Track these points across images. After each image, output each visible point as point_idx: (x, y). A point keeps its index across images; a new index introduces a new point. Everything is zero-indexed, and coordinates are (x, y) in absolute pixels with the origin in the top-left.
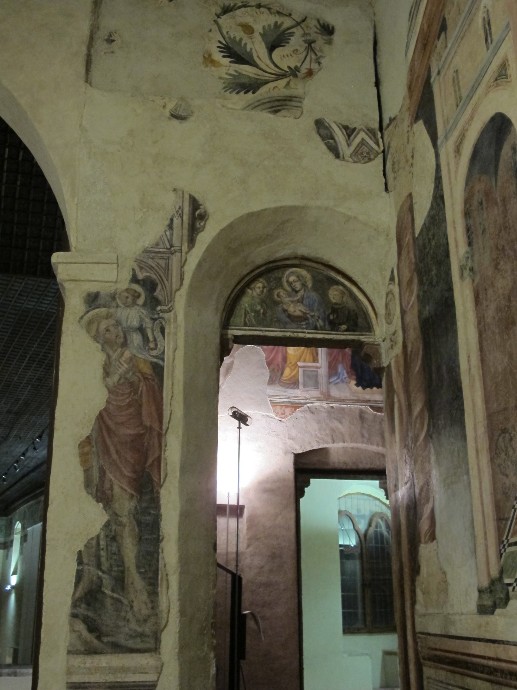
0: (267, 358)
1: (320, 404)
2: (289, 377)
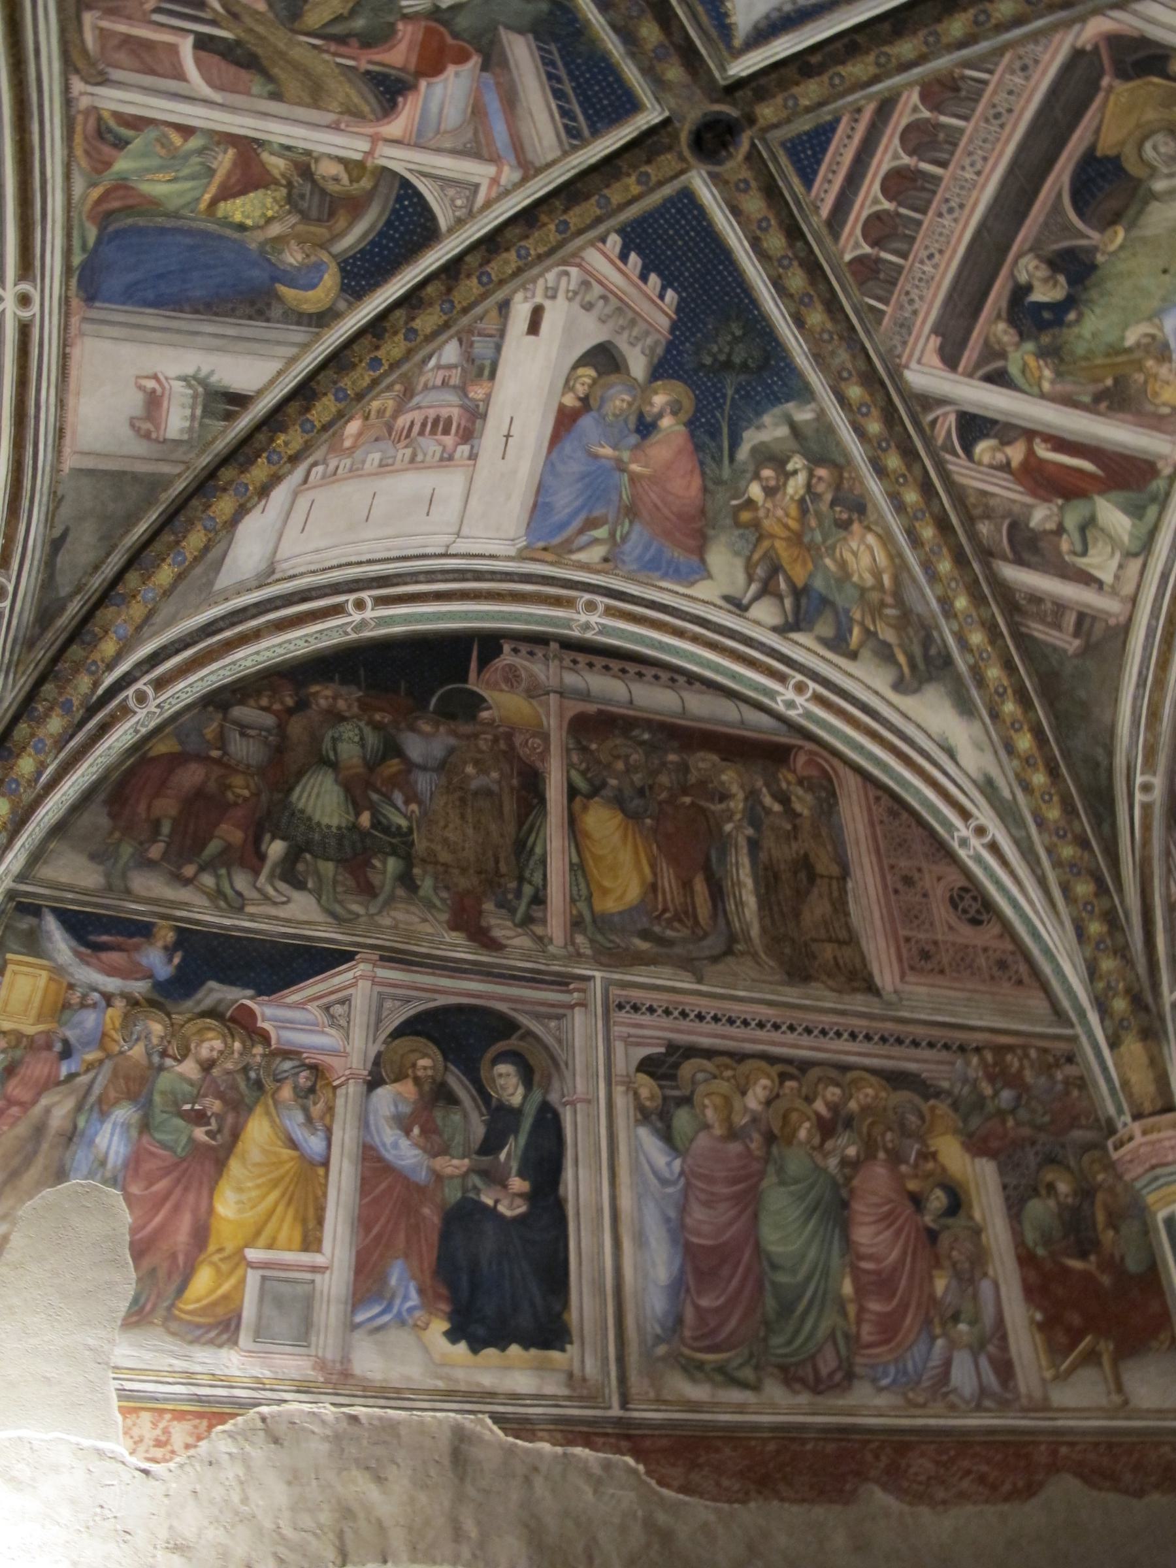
0: (133, 1231)
1: (306, 1407)
2: (204, 1302)
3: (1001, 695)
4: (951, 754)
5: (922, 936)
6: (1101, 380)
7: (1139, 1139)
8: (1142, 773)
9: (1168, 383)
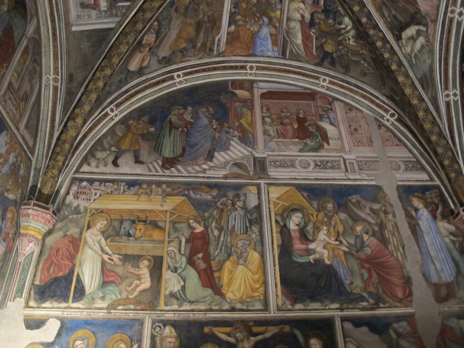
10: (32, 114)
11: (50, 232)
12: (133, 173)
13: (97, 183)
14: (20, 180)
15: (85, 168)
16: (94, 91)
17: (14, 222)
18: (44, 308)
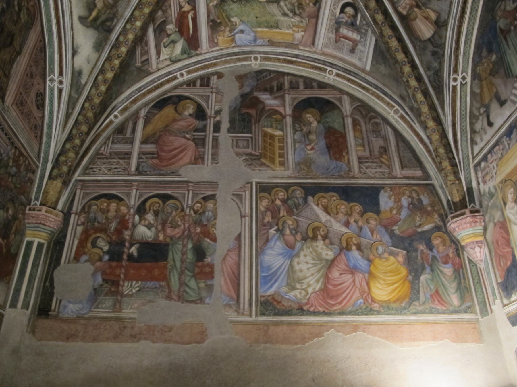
3: (118, 57)
4: (75, 53)
5: (25, 97)
6: (218, 18)
7: (43, 212)
8: (118, 112)
9: (224, 36)
10: (401, 154)
11: (485, 229)
12: (505, 119)
13: (489, 156)
14: (429, 209)
15: (477, 149)
16: (415, 93)
17: (448, 242)
18: (514, 302)
